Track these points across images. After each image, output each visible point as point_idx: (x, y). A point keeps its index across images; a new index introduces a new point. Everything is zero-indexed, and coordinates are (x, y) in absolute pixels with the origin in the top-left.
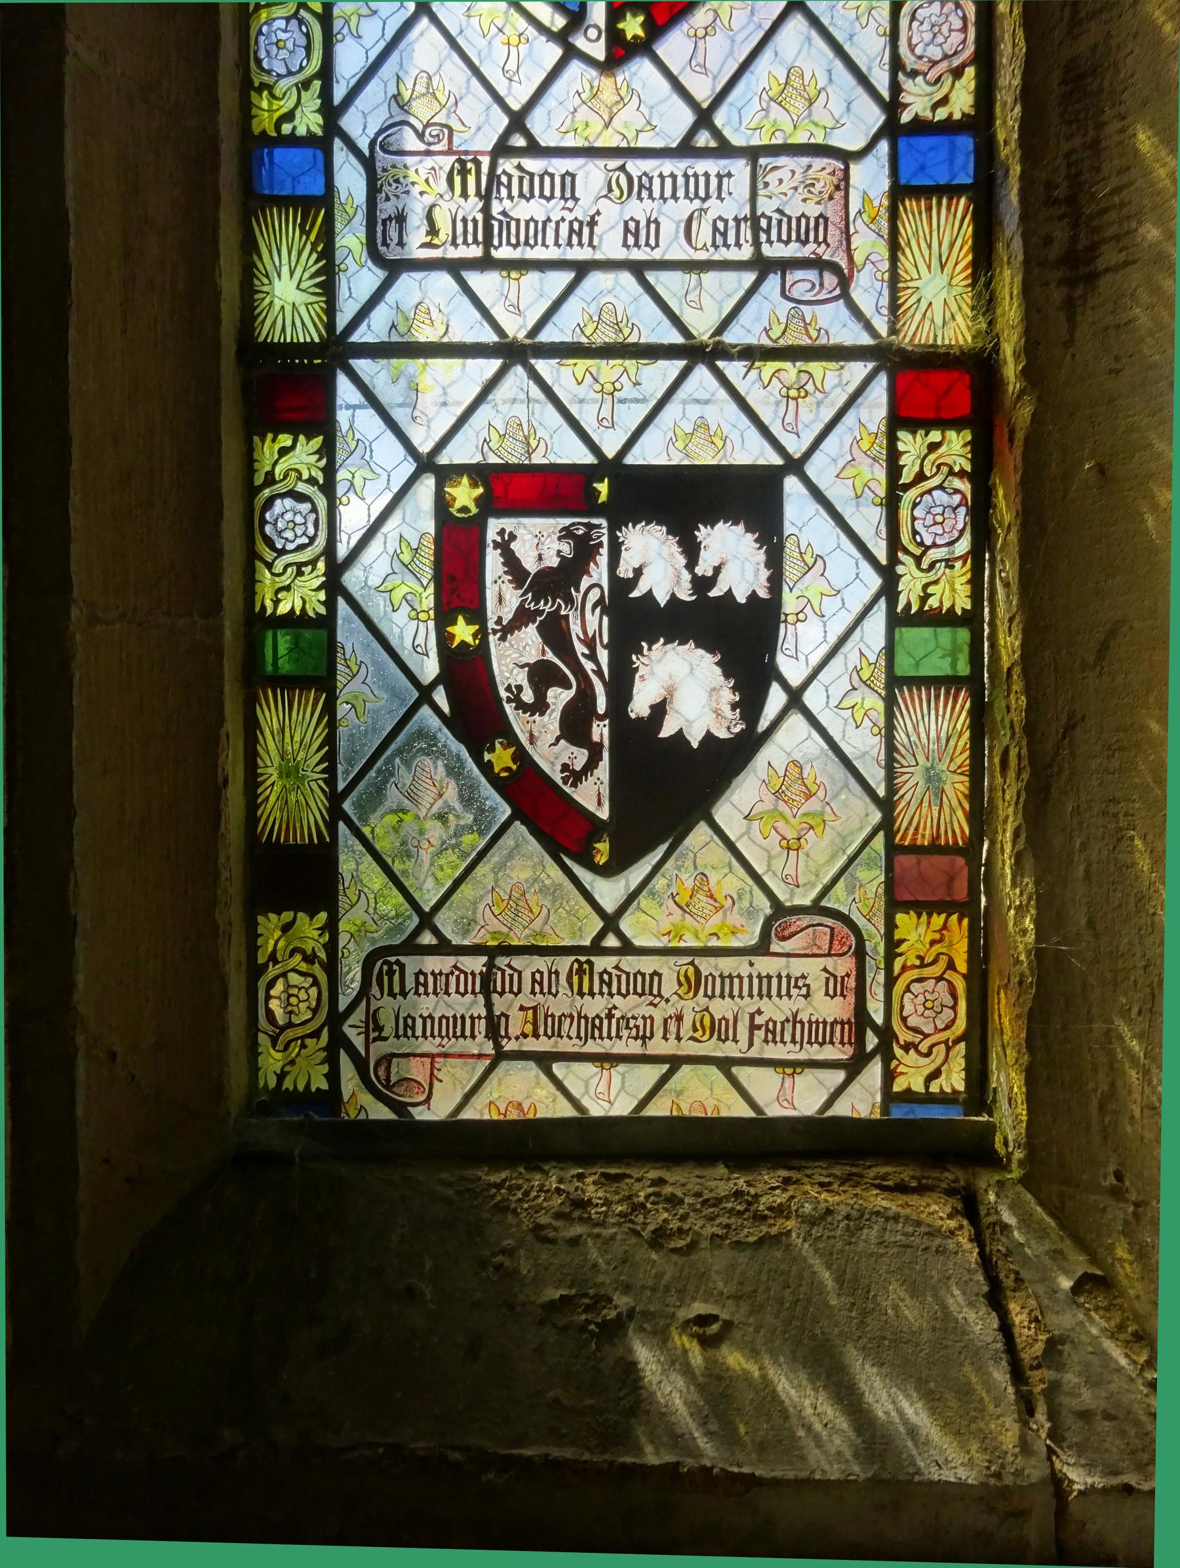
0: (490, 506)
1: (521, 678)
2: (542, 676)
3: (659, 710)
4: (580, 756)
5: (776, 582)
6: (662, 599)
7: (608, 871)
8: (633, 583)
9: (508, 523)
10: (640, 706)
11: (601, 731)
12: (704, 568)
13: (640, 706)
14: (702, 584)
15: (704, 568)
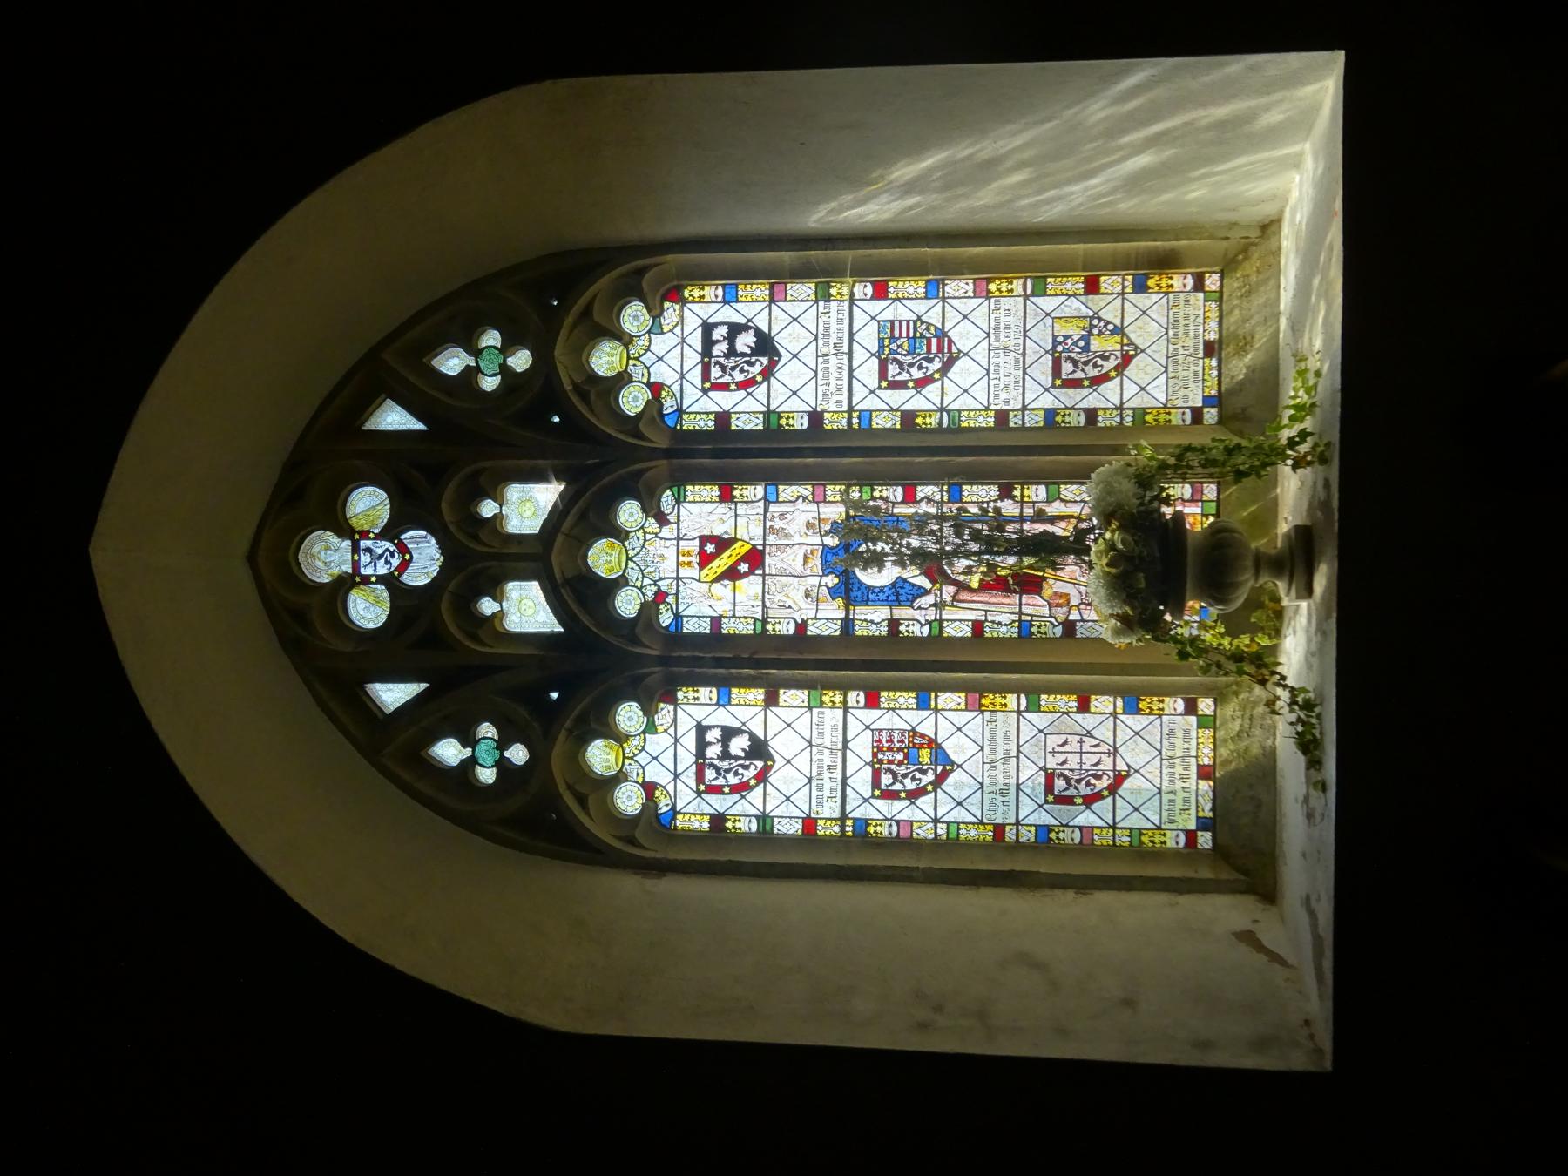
0: (704, 784)
1: (737, 778)
2: (736, 774)
3: (743, 750)
4: (752, 767)
5: (718, 726)
6: (721, 749)
7: (774, 762)
8: (718, 755)
9: (706, 780)
10: (742, 754)
11: (747, 763)
12: (715, 741)
13: (742, 754)
14: (718, 741)
15: (715, 741)
